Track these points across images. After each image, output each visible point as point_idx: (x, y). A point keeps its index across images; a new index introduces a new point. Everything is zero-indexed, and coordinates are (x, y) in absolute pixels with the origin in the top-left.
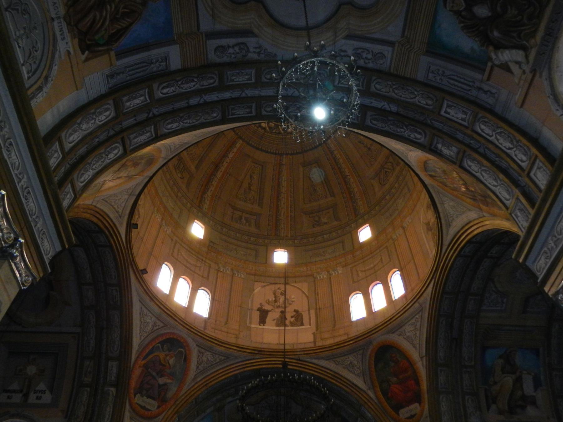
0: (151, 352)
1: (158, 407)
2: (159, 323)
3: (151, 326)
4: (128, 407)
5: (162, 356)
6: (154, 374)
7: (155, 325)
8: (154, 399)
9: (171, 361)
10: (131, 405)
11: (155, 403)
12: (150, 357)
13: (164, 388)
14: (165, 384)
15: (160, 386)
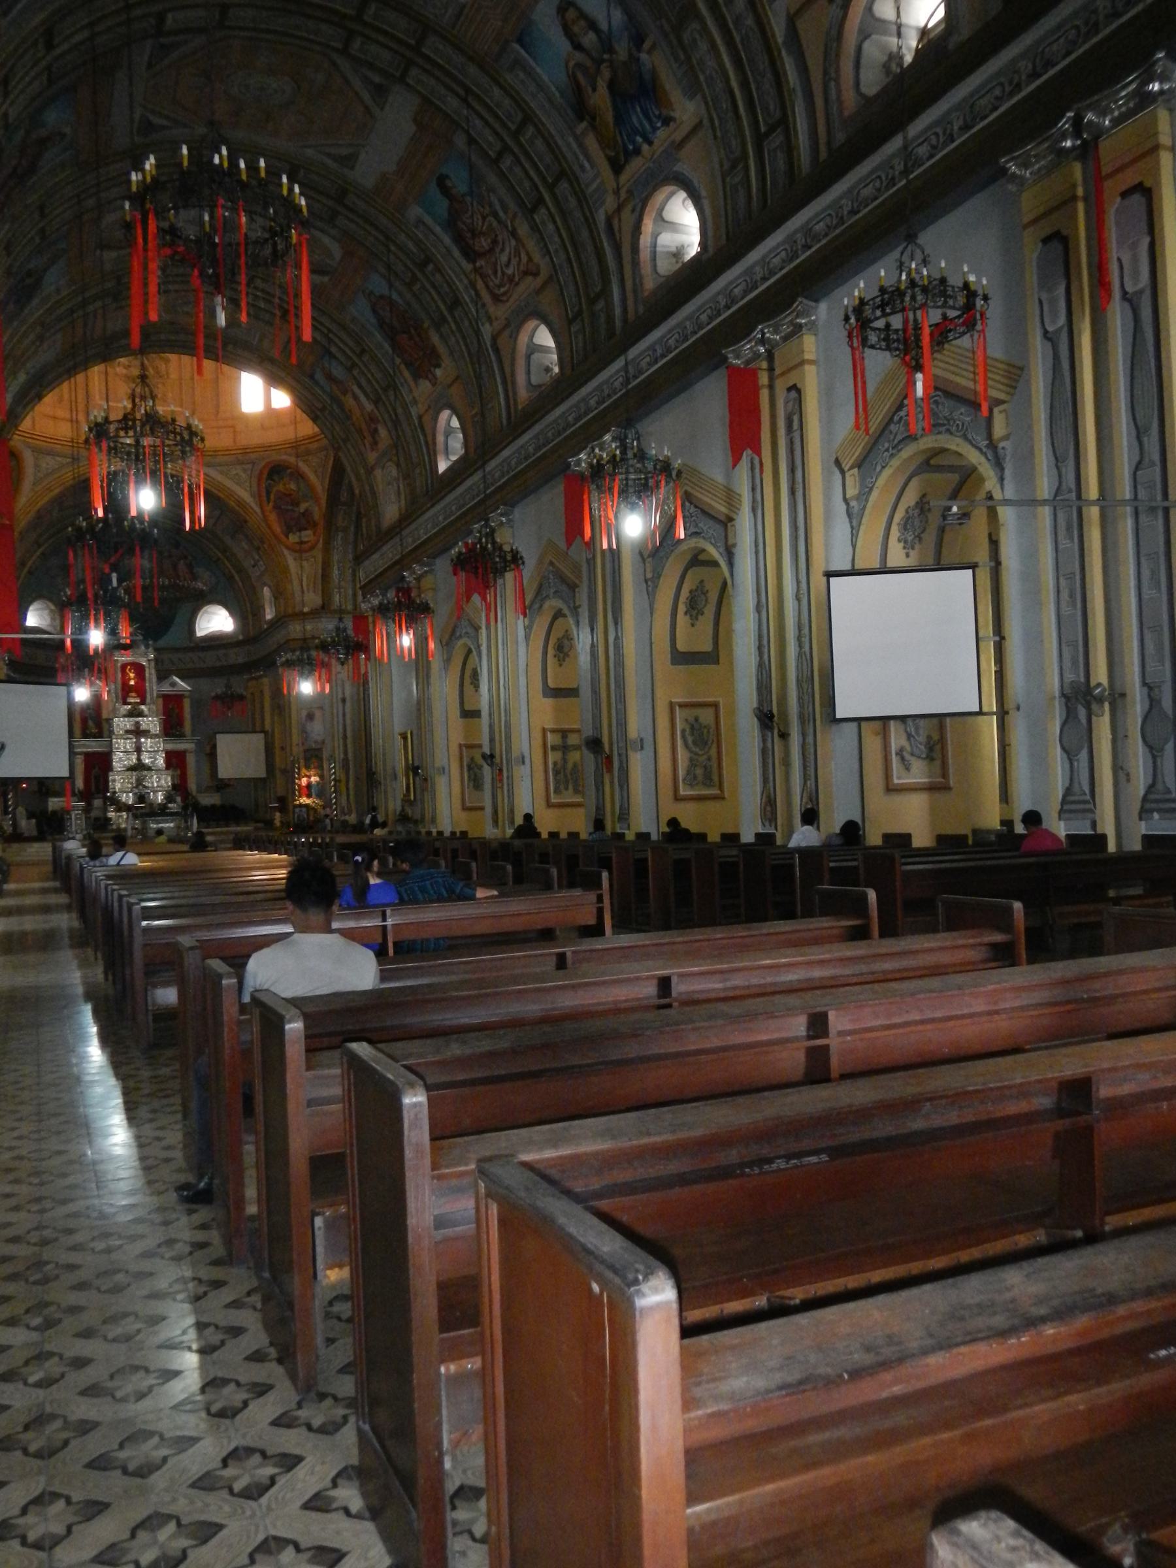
0: (268, 493)
1: (314, 534)
2: (246, 467)
3: (244, 475)
4: (286, 552)
5: (281, 487)
6: (290, 508)
7: (245, 470)
8: (306, 529)
9: (293, 486)
10: (288, 548)
11: (309, 532)
12: (272, 496)
13: (307, 514)
14: (307, 510)
15: (303, 514)
